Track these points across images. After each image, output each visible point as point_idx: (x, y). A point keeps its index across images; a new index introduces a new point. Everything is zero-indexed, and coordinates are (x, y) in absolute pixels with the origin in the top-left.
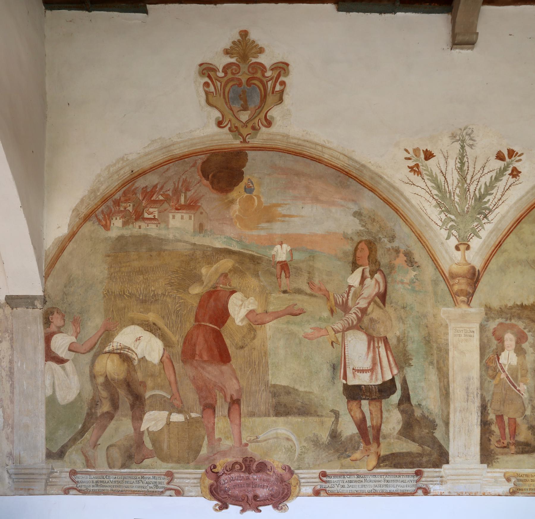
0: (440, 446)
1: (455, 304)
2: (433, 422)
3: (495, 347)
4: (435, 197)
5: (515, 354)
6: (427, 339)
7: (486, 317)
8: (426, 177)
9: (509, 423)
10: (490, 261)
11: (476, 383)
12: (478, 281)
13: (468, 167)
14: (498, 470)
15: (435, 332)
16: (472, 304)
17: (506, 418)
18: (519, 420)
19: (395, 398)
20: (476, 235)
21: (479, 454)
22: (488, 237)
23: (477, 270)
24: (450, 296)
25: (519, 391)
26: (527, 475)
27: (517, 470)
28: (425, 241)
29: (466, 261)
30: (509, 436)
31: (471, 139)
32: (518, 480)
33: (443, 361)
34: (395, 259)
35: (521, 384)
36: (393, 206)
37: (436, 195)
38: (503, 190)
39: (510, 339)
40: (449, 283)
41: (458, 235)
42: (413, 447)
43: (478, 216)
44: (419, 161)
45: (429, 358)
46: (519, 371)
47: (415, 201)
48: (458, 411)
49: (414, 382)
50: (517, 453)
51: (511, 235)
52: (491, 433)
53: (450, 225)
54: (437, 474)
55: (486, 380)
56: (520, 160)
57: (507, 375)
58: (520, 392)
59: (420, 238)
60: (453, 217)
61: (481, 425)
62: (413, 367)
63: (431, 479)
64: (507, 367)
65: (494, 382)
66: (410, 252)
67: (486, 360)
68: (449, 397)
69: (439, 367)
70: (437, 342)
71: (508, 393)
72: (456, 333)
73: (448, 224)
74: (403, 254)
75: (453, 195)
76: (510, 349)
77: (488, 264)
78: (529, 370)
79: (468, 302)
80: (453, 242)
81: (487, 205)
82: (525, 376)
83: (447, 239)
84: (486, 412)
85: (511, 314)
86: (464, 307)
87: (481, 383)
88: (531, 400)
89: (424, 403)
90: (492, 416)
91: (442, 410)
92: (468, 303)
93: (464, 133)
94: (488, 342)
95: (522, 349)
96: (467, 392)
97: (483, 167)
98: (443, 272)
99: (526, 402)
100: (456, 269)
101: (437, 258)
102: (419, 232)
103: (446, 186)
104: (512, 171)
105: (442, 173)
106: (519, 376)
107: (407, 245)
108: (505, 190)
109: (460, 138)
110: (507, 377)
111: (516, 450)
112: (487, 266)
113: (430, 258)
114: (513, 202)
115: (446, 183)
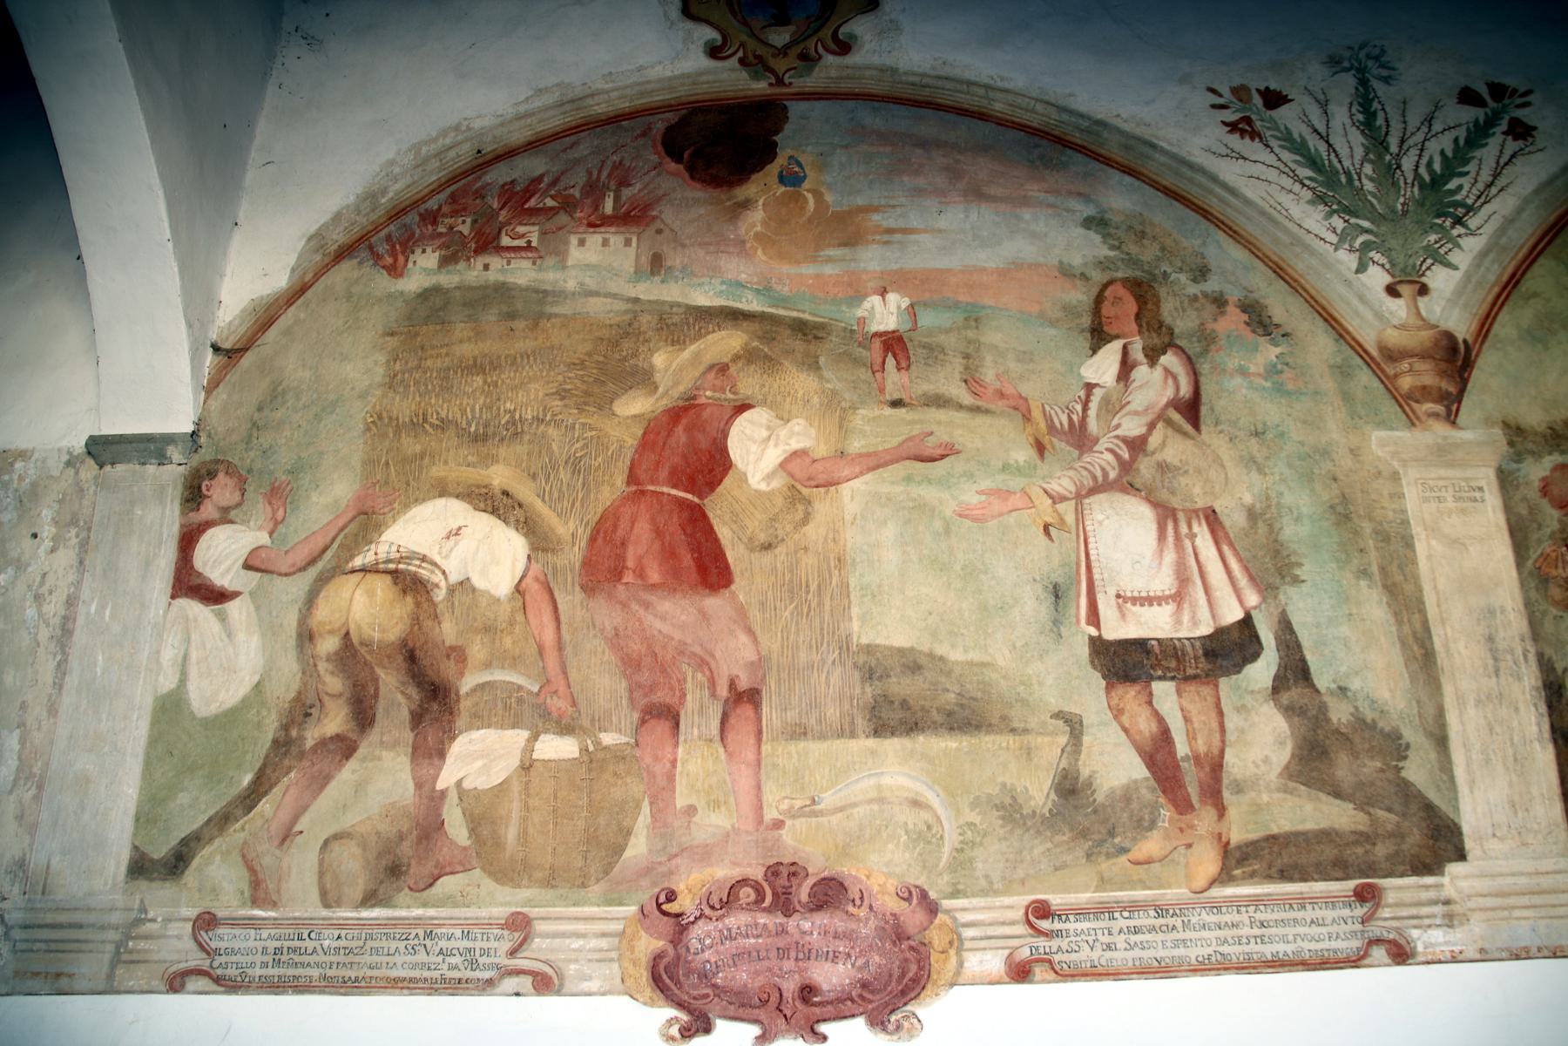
0: (1429, 808)
1: (1411, 420)
2: (1395, 736)
6: (1340, 509)
7: (1511, 450)
8: (1274, 143)
10: (1494, 318)
11: (1514, 624)
15: (1362, 492)
16: (1462, 418)
19: (1262, 671)
20: (1441, 263)
24: (1393, 401)
28: (1296, 277)
29: (1423, 319)
31: (1382, 66)
33: (1400, 567)
34: (1215, 320)
36: (1194, 204)
37: (1310, 178)
38: (1494, 165)
40: (1383, 371)
41: (1390, 262)
42: (1339, 816)
43: (1439, 221)
44: (1251, 109)
45: (1355, 561)
47: (1252, 191)
48: (1472, 702)
49: (1318, 626)
53: (1360, 239)
54: (1432, 894)
55: (1544, 614)
56: (1527, 104)
59: (1279, 271)
60: (1366, 224)
61: (1555, 742)
62: (1309, 583)
63: (1414, 911)
66: (1257, 302)
67: (1536, 561)
68: (1435, 663)
69: (1389, 583)
72: (1427, 494)
73: (1354, 238)
74: (1236, 306)
75: (1355, 177)
77: (1491, 324)
80: (1377, 278)
81: (1458, 197)
86: (1441, 429)
89: (1355, 684)
91: (1418, 702)
92: (1451, 418)
93: (1362, 55)
96: (1491, 650)
98: (1360, 346)
100: (1394, 338)
103: (1335, 161)
105: (1319, 134)
107: (1245, 288)
112: (1488, 331)
113: (1316, 315)
115: (1333, 155)
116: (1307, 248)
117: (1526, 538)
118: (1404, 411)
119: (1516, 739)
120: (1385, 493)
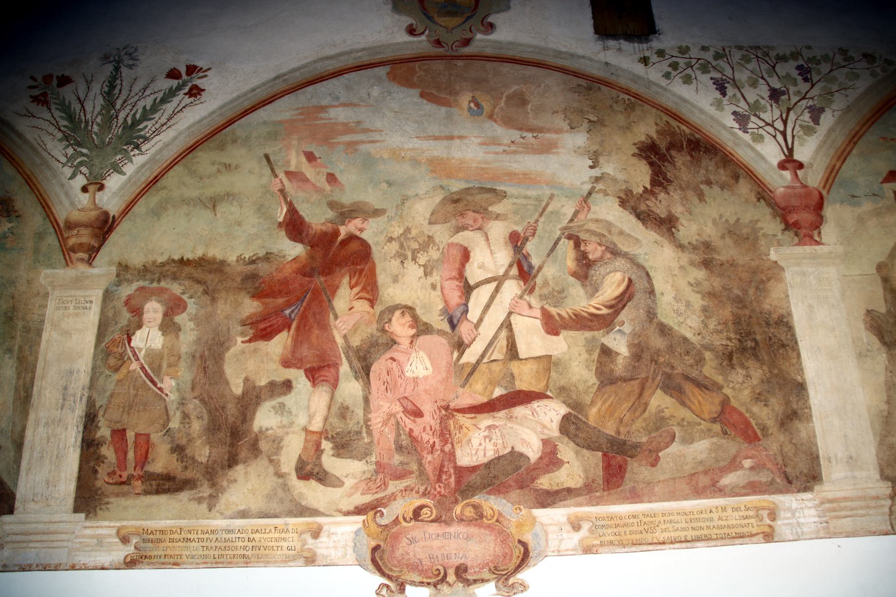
3: (125, 322)
4: (62, 128)
5: (161, 332)
6: (9, 314)
7: (116, 279)
9: (135, 442)
10: (136, 203)
11: (84, 378)
12: (111, 229)
13: (120, 91)
14: (106, 523)
15: (25, 304)
16: (94, 263)
17: (130, 435)
18: (155, 437)
21: (73, 495)
22: (137, 172)
23: (111, 217)
25: (160, 389)
26: (162, 532)
27: (143, 523)
28: (36, 183)
29: (95, 205)
30: (134, 465)
31: (132, 59)
32: (144, 541)
35: (167, 379)
37: (65, 126)
38: (171, 113)
39: (153, 310)
40: (62, 235)
45: (7, 344)
46: (166, 358)
48: (43, 424)
50: (147, 493)
51: (176, 167)
52: (100, 459)
53: (78, 160)
55: (101, 374)
56: (206, 76)
57: (142, 364)
58: (162, 392)
61: (82, 447)
64: (143, 352)
65: (116, 377)
66: (10, 198)
67: (108, 343)
68: (30, 401)
70: (24, 319)
71: (139, 393)
72: (60, 305)
75: (90, 124)
76: (152, 324)
77: (133, 206)
78: (184, 356)
79: (89, 259)
81: (142, 133)
82: (176, 366)
83: (71, 178)
84: (94, 424)
85: (161, 273)
86: (82, 268)
87: (92, 379)
88: (183, 404)
90: (104, 431)
91: (13, 423)
92: (90, 262)
93: (122, 53)
94: (114, 315)
95: (174, 324)
96: (63, 394)
97: (145, 89)
98: (56, 221)
99: (172, 408)
100: (76, 216)
101: (50, 204)
102: (28, 173)
103: (82, 114)
104: (191, 89)
106: (165, 366)
107: (6, 191)
108: (176, 112)
109: (115, 59)
110: (143, 368)
111: (143, 487)
112: (130, 210)
113: (39, 204)
114: (186, 126)
116: (49, 167)
117: (106, 330)
118: (65, 258)
119: (61, 445)
120: (37, 305)
